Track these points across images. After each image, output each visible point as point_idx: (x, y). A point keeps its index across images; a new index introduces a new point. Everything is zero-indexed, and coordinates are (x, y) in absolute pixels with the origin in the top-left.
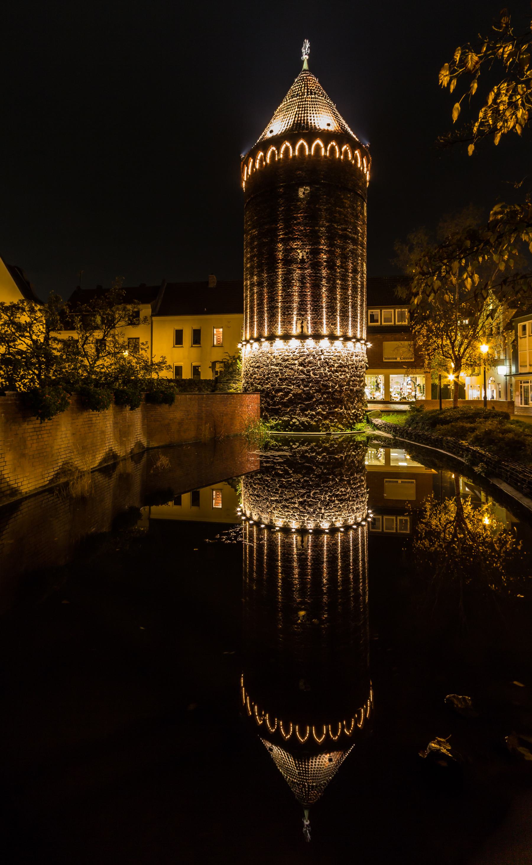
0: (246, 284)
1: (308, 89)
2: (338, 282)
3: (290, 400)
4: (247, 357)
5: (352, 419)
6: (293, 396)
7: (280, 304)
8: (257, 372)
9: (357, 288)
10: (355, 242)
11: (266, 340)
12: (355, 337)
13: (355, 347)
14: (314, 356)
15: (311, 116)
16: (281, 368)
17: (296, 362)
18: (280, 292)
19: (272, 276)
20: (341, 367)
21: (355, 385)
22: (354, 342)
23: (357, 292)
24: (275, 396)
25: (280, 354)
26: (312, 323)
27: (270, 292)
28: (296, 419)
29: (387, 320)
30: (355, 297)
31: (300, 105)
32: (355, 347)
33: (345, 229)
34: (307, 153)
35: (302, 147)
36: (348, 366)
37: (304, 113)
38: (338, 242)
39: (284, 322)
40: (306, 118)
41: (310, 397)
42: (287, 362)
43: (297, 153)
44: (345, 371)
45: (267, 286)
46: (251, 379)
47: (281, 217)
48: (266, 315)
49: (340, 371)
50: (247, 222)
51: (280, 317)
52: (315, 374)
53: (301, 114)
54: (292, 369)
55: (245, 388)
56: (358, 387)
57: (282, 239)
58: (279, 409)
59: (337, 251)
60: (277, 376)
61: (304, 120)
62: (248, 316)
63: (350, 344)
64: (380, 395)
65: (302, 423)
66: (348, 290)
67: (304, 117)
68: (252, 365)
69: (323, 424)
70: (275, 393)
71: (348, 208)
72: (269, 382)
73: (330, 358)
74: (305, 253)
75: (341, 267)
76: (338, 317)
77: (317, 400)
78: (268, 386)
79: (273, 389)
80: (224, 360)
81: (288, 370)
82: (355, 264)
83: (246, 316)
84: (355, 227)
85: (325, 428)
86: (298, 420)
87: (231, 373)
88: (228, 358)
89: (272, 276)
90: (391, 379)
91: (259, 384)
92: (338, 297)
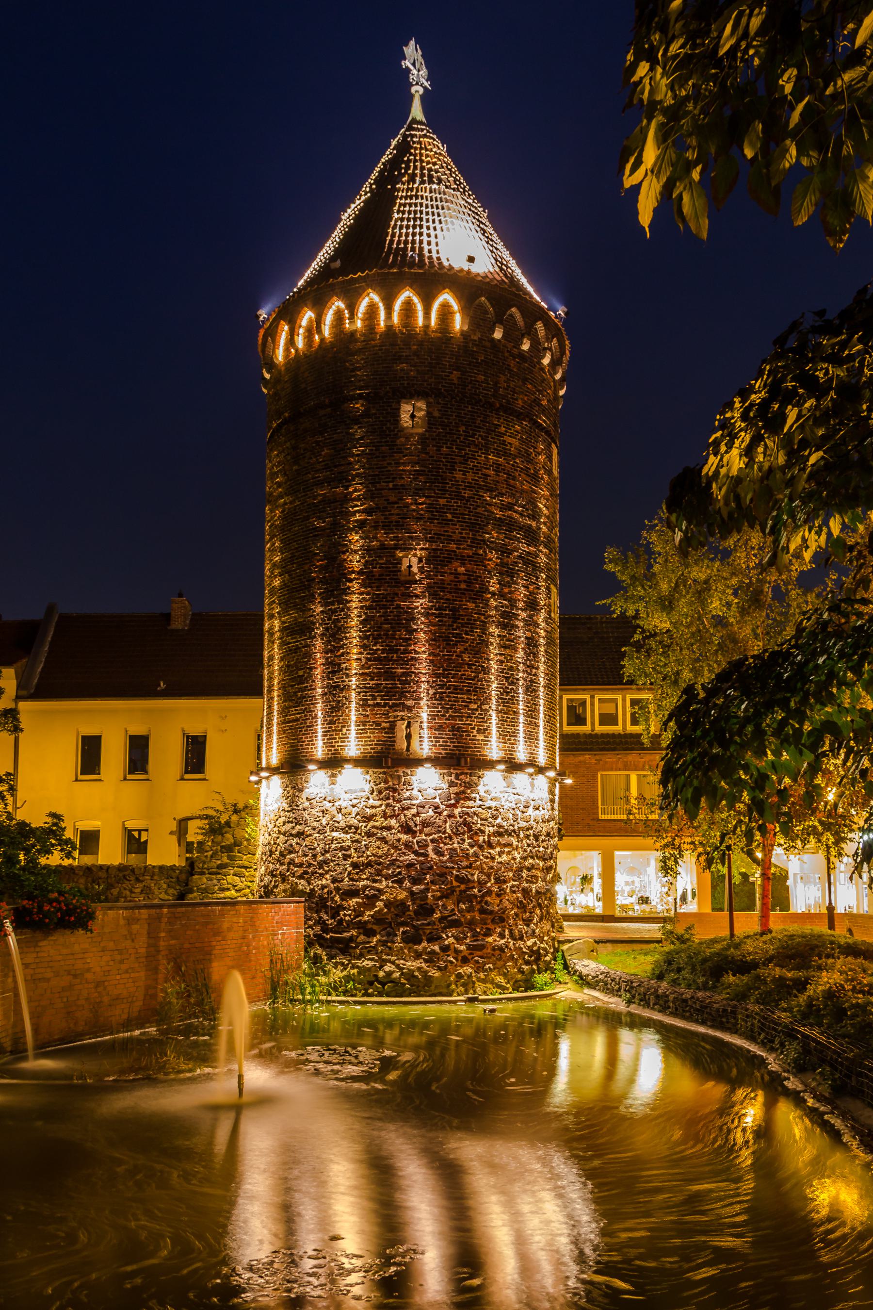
0: (271, 628)
1: (422, 168)
2: (493, 629)
3: (378, 919)
4: (271, 808)
5: (527, 963)
6: (386, 906)
7: (354, 679)
8: (297, 848)
9: (536, 646)
10: (532, 536)
11: (320, 768)
12: (532, 763)
13: (532, 785)
14: (437, 807)
15: (429, 235)
16: (357, 837)
17: (393, 822)
18: (355, 651)
19: (334, 611)
20: (500, 835)
21: (533, 879)
22: (531, 775)
23: (535, 655)
24: (341, 907)
25: (355, 802)
26: (430, 728)
27: (331, 651)
28: (393, 963)
29: (608, 719)
30: (531, 667)
31: (405, 205)
32: (532, 785)
33: (510, 507)
34: (420, 322)
35: (408, 309)
36: (515, 833)
37: (414, 227)
38: (493, 535)
39: (364, 723)
40: (417, 238)
41: (426, 910)
42: (371, 824)
43: (396, 319)
44: (509, 845)
45: (322, 635)
46: (282, 864)
47: (358, 469)
48: (319, 706)
49: (499, 844)
50: (274, 475)
51: (353, 712)
52: (439, 853)
53: (408, 227)
54: (383, 839)
55: (266, 887)
56: (540, 883)
57: (361, 524)
58: (351, 939)
59: (490, 555)
60: (346, 857)
61: (413, 242)
62: (276, 707)
63: (520, 779)
64: (590, 900)
65: (410, 976)
66: (515, 649)
67: (414, 234)
68: (283, 829)
69: (459, 976)
70: (342, 899)
71: (516, 457)
72: (327, 872)
73: (475, 814)
74: (415, 560)
75: (502, 595)
76: (494, 714)
77: (442, 919)
78: (324, 882)
79: (337, 889)
80: (212, 813)
81: (374, 843)
82: (531, 588)
83: (270, 707)
84: (533, 503)
85: (463, 985)
86: (398, 966)
87: (229, 849)
88: (221, 808)
89: (334, 611)
90: (616, 861)
91: (301, 877)
92: (494, 666)
